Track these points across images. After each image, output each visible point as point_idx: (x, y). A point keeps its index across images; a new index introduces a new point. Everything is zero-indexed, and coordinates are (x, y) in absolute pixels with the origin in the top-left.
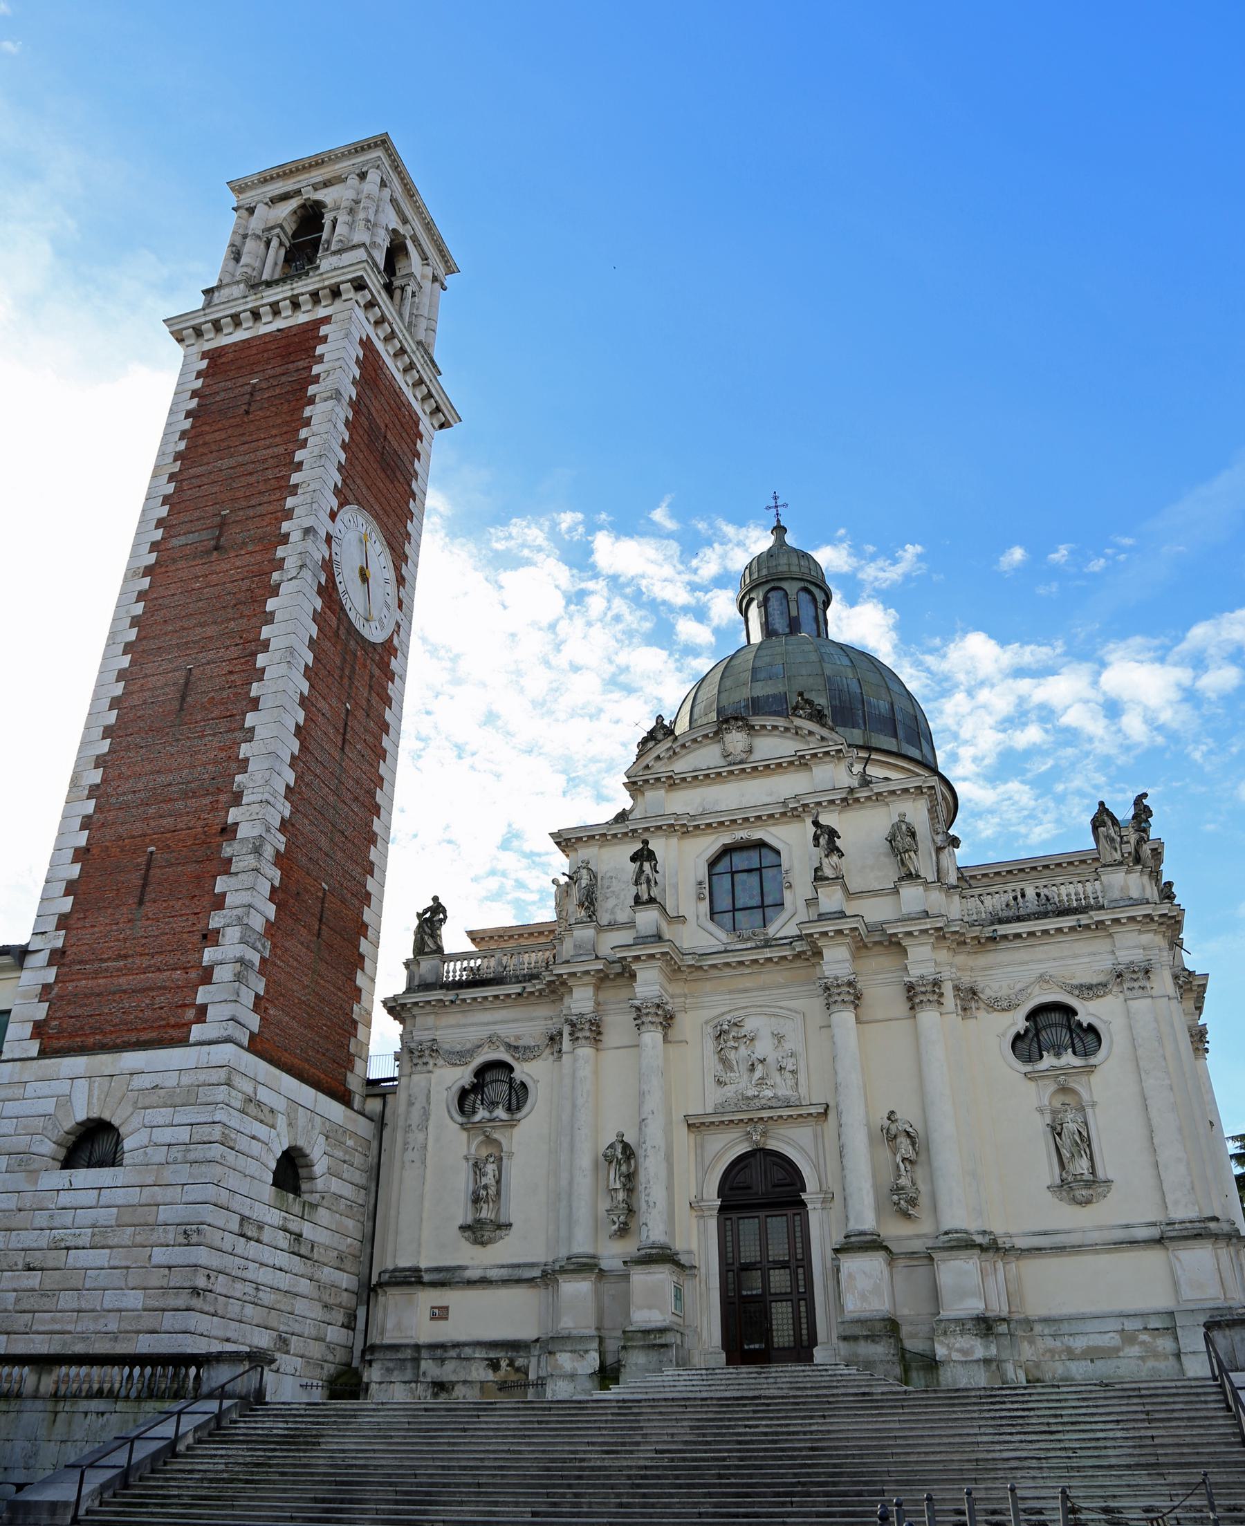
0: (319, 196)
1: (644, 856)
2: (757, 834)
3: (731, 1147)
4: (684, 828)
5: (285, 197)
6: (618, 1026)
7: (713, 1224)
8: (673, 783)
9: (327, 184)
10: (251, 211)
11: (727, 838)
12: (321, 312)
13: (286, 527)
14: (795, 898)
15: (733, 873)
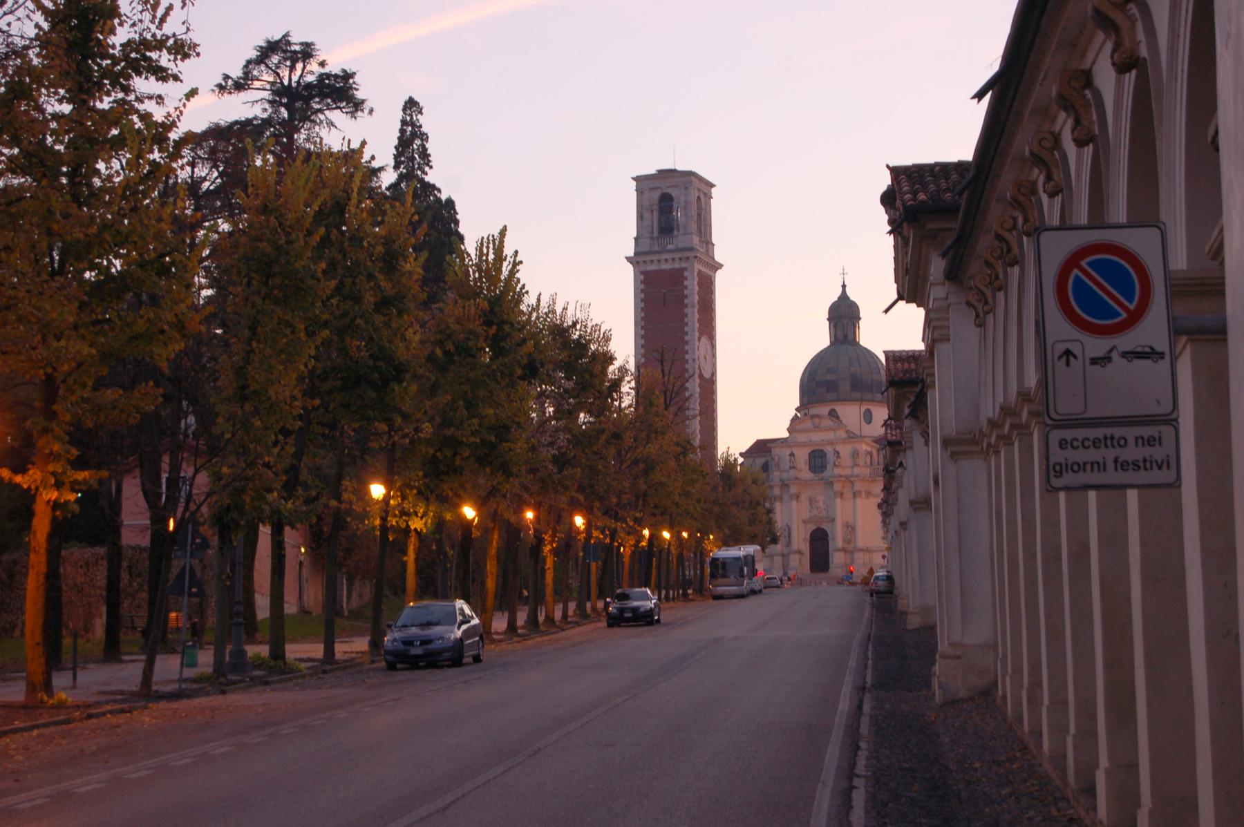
0: (670, 191)
1: (792, 455)
2: (822, 448)
3: (812, 527)
4: (803, 445)
5: (655, 188)
6: (786, 497)
7: (808, 545)
8: (800, 431)
9: (672, 187)
10: (642, 192)
11: (813, 449)
12: (684, 265)
13: (687, 357)
14: (829, 466)
15: (815, 457)
